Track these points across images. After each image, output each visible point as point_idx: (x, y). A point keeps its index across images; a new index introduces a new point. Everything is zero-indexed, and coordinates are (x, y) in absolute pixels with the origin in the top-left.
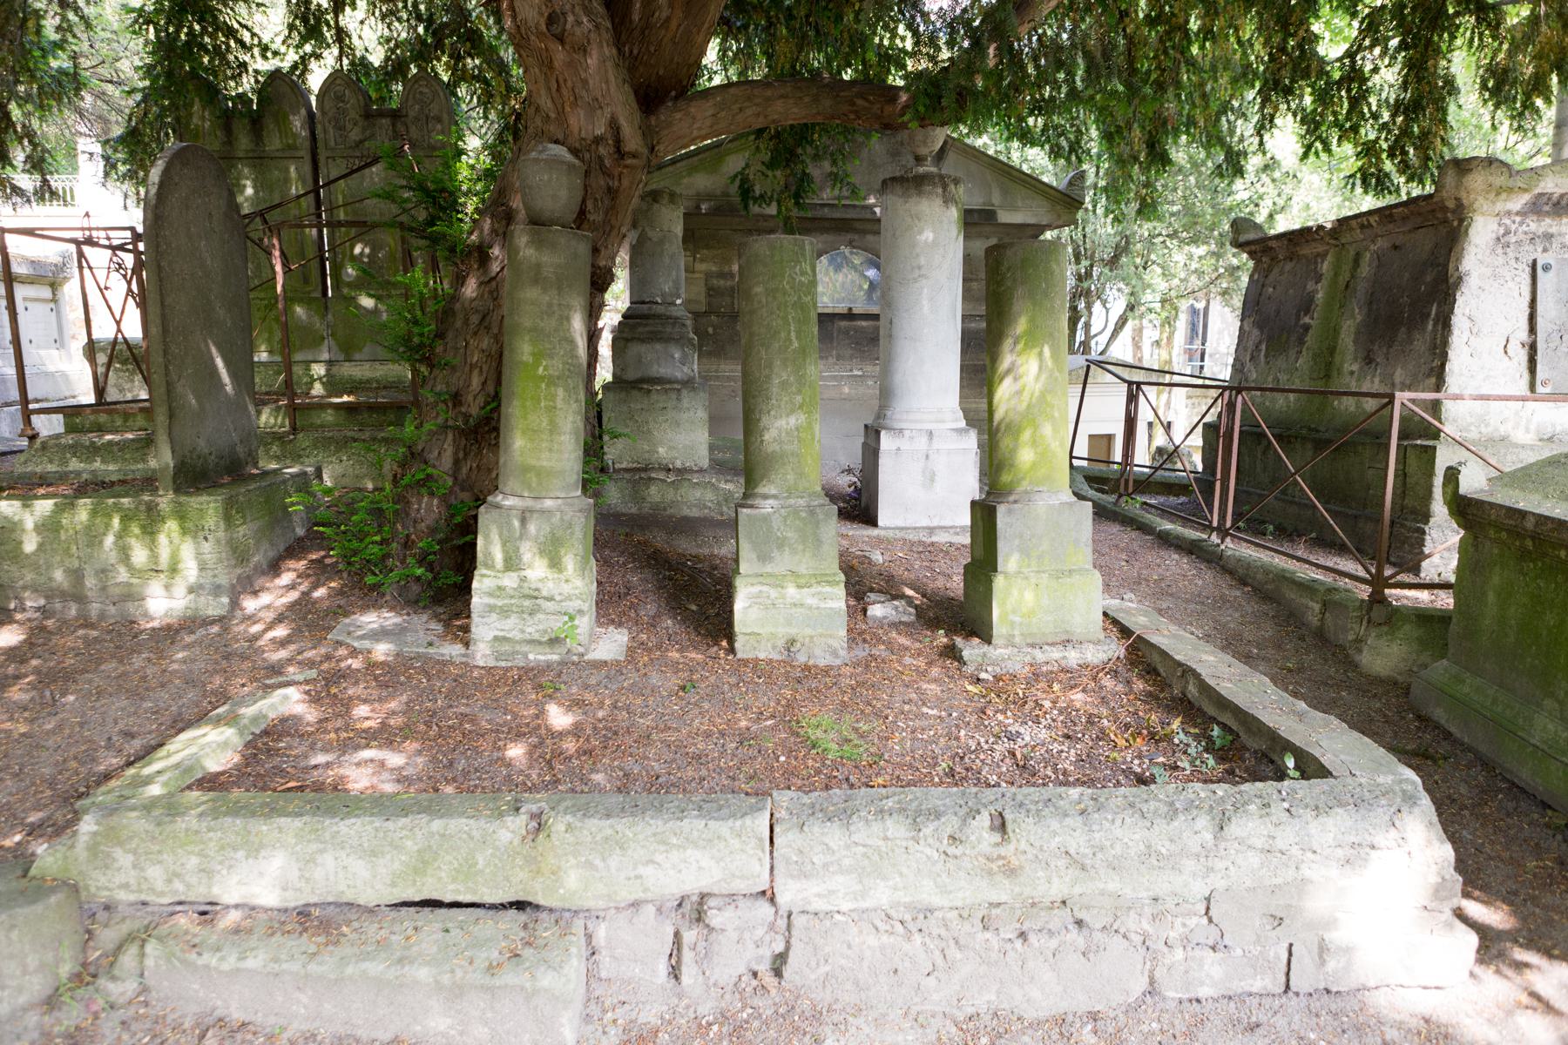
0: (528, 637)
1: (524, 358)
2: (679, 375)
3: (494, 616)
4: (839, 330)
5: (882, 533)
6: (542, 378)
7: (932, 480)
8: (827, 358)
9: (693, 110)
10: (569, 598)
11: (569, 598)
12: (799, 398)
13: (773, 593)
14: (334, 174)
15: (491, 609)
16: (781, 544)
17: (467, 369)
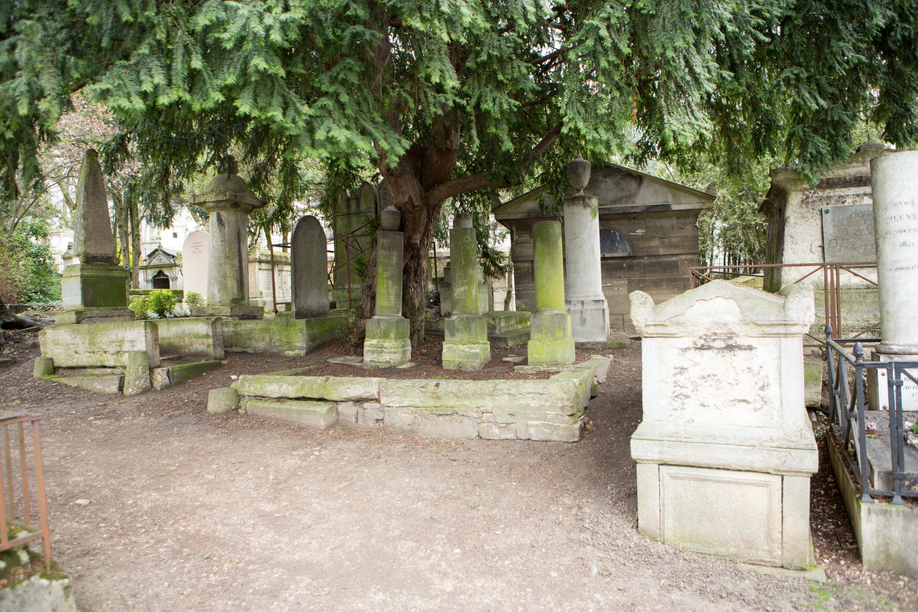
7: (584, 322)
10: (391, 348)
11: (391, 348)
12: (465, 281)
13: (455, 347)
15: (369, 351)
16: (458, 330)
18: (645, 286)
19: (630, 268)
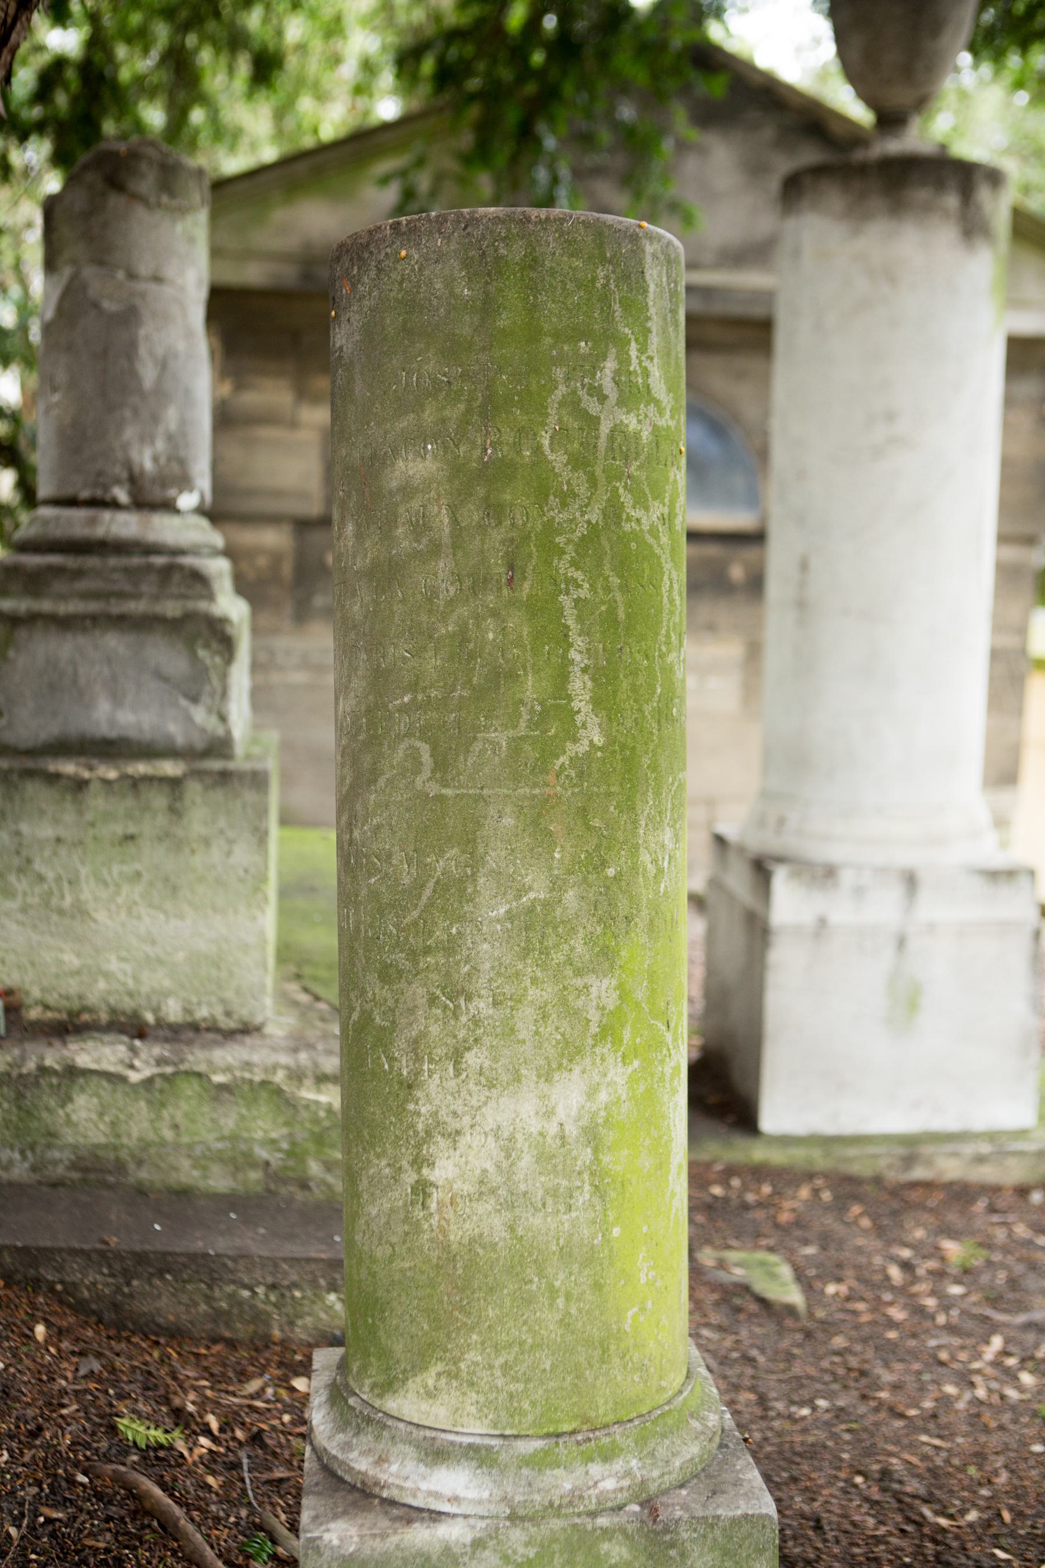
2: (176, 732)
5: (776, 1157)
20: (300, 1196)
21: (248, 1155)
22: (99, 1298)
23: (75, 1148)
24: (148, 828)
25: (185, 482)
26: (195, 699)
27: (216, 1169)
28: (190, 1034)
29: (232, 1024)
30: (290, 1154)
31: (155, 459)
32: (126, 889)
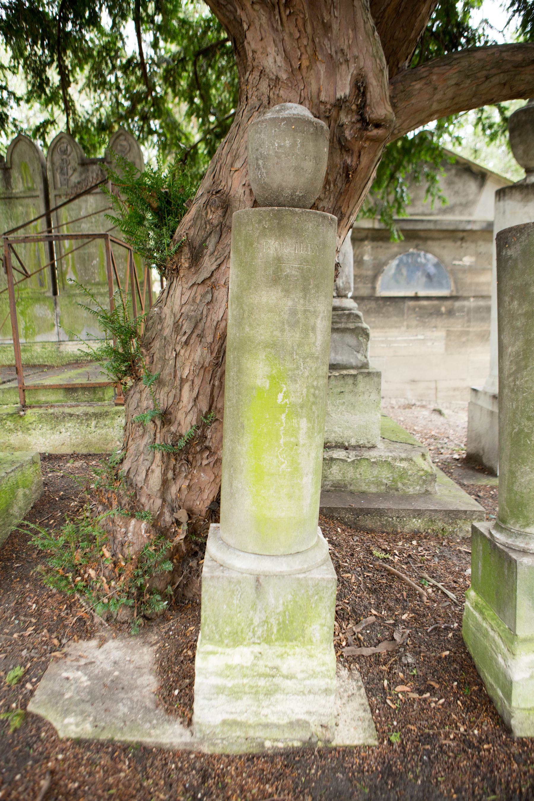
0: (264, 720)
1: (259, 382)
2: (353, 361)
3: (222, 698)
4: (409, 308)
6: (283, 408)
8: (400, 327)
9: (435, 78)
10: (313, 675)
11: (313, 675)
14: (59, 203)
17: (178, 382)
18: (468, 340)
19: (450, 313)
20: (396, 493)
21: (381, 482)
22: (350, 521)
23: (333, 481)
24: (347, 389)
25: (349, 289)
26: (358, 352)
27: (372, 486)
28: (359, 449)
29: (370, 446)
30: (393, 481)
31: (343, 283)
32: (340, 407)
